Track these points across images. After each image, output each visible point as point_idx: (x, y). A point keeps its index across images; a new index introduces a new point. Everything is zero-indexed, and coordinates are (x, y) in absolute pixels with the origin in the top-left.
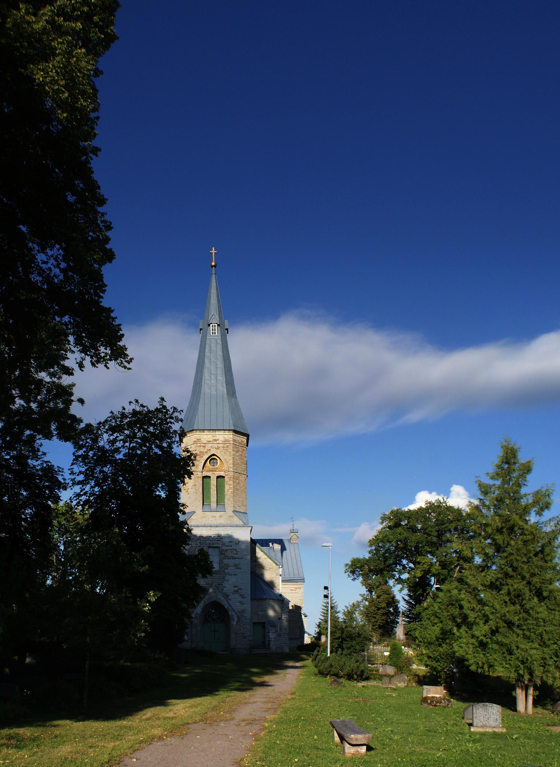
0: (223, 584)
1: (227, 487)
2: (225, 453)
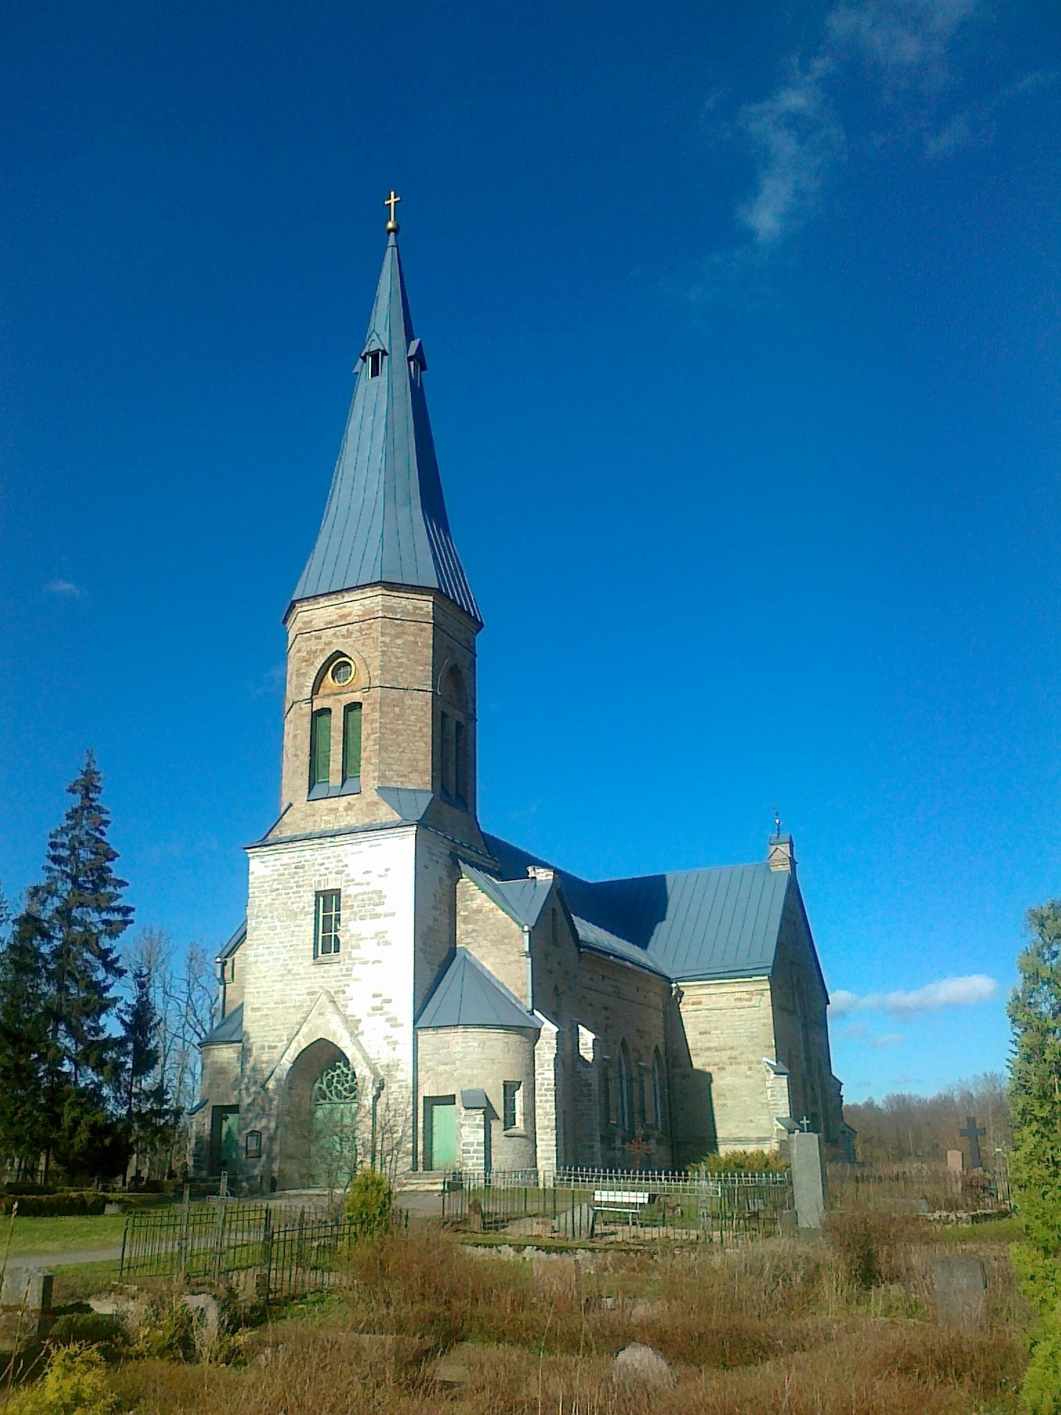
0: (346, 989)
1: (365, 729)
2: (363, 645)
